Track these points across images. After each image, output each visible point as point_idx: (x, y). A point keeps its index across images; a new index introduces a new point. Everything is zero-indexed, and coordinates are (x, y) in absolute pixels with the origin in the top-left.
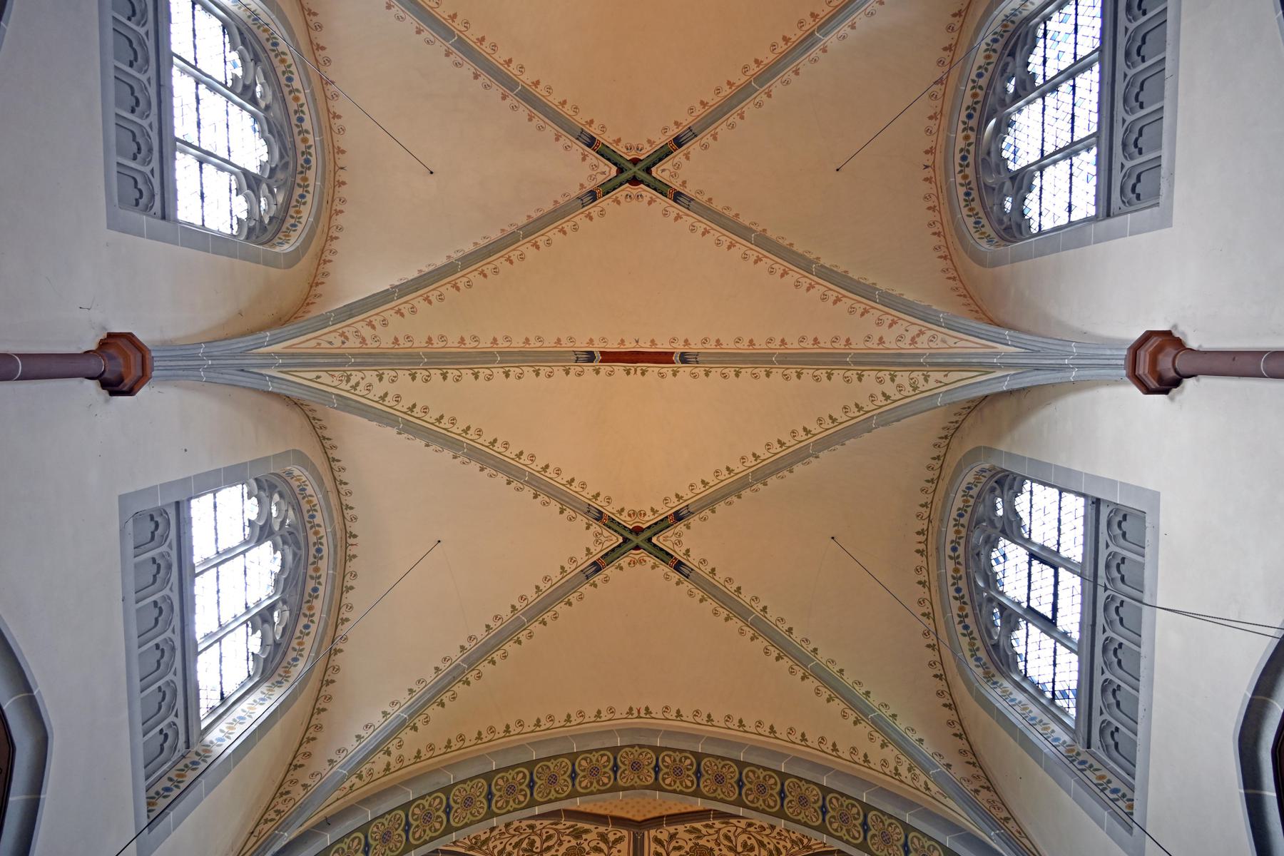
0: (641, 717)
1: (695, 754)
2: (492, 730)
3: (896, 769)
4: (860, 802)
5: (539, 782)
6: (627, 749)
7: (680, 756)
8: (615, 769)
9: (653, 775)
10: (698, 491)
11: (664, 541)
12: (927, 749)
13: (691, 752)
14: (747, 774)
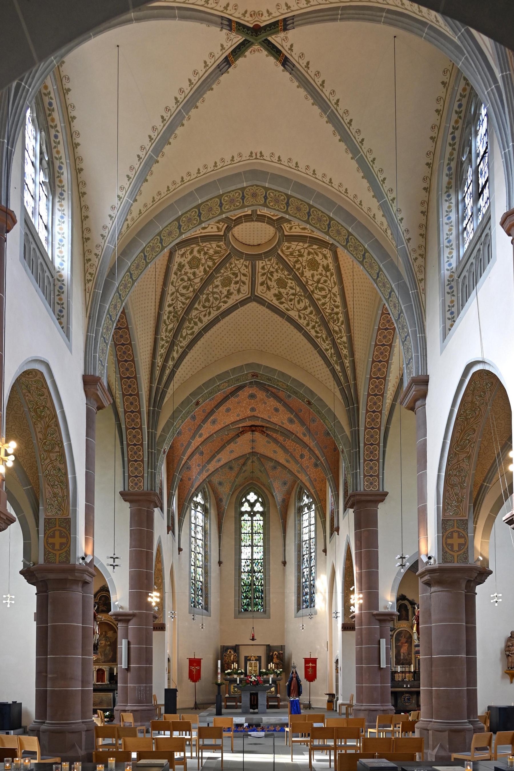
0: (257, 159)
2: (174, 183)
3: (386, 229)
4: (364, 247)
5: (203, 213)
8: (243, 198)
10: (302, 6)
12: (402, 227)
14: (313, 211)
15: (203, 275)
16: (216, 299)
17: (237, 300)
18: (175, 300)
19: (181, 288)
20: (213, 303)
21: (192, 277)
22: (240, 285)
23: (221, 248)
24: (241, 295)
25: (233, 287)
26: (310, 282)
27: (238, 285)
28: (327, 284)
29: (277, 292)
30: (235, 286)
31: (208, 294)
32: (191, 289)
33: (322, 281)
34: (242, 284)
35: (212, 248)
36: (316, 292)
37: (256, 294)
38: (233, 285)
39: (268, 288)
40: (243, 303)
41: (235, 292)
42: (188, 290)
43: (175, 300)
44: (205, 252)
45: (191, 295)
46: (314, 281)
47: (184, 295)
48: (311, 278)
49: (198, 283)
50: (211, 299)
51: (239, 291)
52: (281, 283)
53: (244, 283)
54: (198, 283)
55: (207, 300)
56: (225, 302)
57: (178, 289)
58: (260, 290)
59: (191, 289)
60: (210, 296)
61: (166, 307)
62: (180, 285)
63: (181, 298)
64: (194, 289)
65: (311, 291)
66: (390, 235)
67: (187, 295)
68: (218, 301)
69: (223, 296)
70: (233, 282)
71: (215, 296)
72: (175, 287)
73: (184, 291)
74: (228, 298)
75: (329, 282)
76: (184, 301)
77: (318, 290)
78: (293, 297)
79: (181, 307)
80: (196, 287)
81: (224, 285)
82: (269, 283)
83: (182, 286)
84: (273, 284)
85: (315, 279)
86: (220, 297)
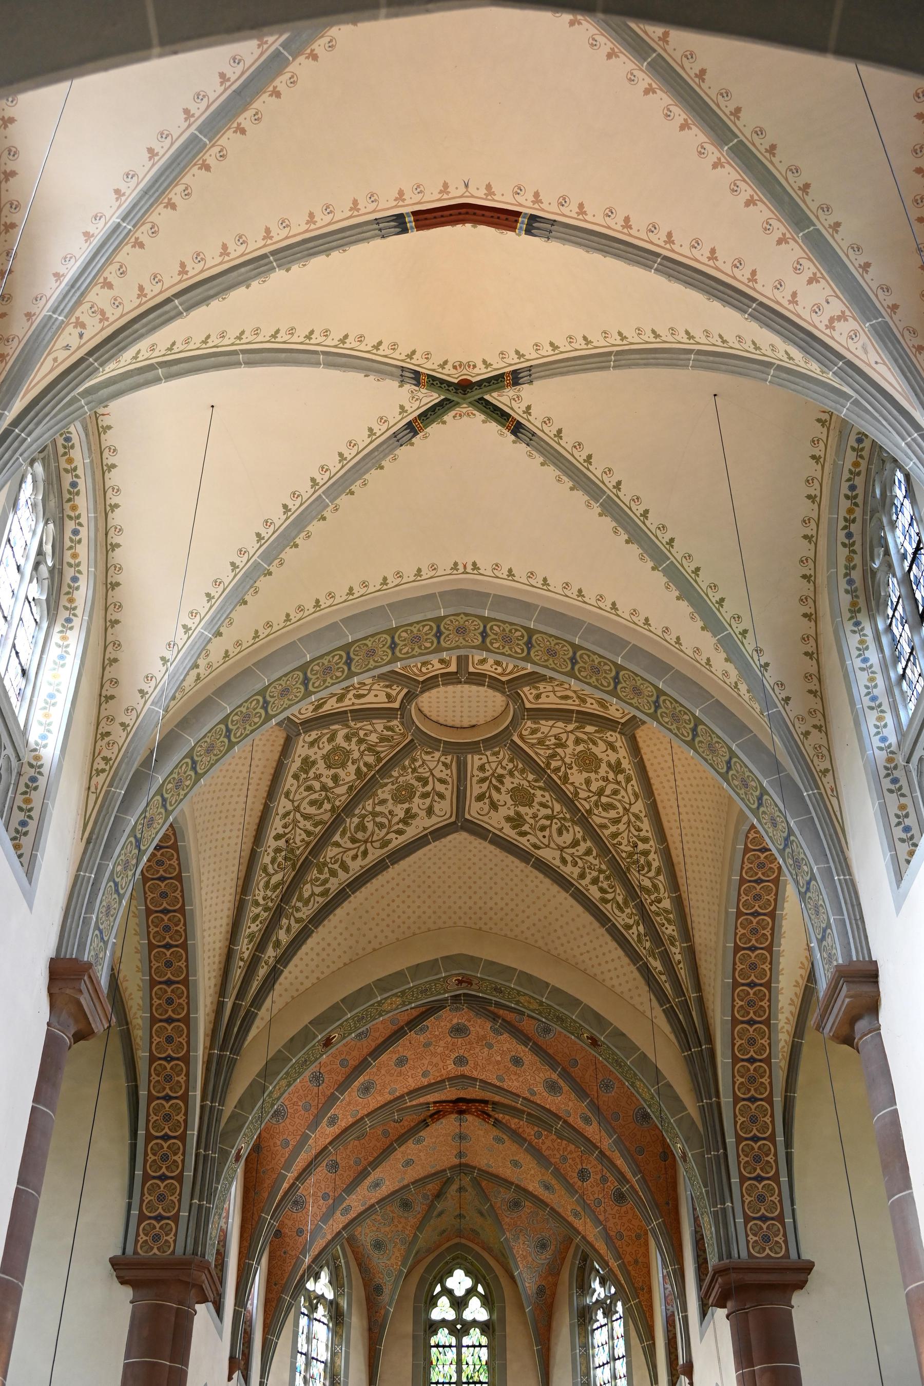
1: (527, 629)
4: (693, 715)
6: (452, 618)
7: (509, 627)
9: (480, 639)
11: (502, 398)
12: (770, 677)
13: (523, 627)
16: (381, 826)
17: (425, 829)
18: (291, 827)
19: (305, 804)
20: (373, 834)
22: (433, 800)
24: (434, 819)
26: (583, 794)
27: (428, 801)
28: (619, 797)
29: (512, 813)
30: (422, 801)
31: (363, 817)
32: (327, 806)
33: (608, 792)
34: (436, 798)
36: (596, 812)
37: (467, 816)
38: (416, 800)
40: (439, 833)
41: (423, 814)
42: (320, 807)
43: (291, 827)
45: (326, 817)
47: (311, 818)
48: (584, 787)
49: (343, 795)
50: (370, 826)
51: (430, 811)
52: (521, 796)
53: (441, 796)
54: (343, 795)
55: (362, 827)
56: (400, 832)
57: (299, 806)
58: (475, 810)
59: (327, 806)
60: (366, 819)
62: (304, 798)
63: (303, 823)
64: (333, 807)
65: (587, 811)
66: (746, 692)
67: (317, 818)
68: (384, 831)
69: (395, 819)
70: (418, 794)
71: (378, 819)
72: (293, 801)
73: (312, 810)
75: (623, 793)
76: (311, 828)
78: (548, 823)
80: (337, 803)
81: (398, 798)
83: (307, 800)
84: (503, 797)
85: (594, 787)
86: (390, 821)
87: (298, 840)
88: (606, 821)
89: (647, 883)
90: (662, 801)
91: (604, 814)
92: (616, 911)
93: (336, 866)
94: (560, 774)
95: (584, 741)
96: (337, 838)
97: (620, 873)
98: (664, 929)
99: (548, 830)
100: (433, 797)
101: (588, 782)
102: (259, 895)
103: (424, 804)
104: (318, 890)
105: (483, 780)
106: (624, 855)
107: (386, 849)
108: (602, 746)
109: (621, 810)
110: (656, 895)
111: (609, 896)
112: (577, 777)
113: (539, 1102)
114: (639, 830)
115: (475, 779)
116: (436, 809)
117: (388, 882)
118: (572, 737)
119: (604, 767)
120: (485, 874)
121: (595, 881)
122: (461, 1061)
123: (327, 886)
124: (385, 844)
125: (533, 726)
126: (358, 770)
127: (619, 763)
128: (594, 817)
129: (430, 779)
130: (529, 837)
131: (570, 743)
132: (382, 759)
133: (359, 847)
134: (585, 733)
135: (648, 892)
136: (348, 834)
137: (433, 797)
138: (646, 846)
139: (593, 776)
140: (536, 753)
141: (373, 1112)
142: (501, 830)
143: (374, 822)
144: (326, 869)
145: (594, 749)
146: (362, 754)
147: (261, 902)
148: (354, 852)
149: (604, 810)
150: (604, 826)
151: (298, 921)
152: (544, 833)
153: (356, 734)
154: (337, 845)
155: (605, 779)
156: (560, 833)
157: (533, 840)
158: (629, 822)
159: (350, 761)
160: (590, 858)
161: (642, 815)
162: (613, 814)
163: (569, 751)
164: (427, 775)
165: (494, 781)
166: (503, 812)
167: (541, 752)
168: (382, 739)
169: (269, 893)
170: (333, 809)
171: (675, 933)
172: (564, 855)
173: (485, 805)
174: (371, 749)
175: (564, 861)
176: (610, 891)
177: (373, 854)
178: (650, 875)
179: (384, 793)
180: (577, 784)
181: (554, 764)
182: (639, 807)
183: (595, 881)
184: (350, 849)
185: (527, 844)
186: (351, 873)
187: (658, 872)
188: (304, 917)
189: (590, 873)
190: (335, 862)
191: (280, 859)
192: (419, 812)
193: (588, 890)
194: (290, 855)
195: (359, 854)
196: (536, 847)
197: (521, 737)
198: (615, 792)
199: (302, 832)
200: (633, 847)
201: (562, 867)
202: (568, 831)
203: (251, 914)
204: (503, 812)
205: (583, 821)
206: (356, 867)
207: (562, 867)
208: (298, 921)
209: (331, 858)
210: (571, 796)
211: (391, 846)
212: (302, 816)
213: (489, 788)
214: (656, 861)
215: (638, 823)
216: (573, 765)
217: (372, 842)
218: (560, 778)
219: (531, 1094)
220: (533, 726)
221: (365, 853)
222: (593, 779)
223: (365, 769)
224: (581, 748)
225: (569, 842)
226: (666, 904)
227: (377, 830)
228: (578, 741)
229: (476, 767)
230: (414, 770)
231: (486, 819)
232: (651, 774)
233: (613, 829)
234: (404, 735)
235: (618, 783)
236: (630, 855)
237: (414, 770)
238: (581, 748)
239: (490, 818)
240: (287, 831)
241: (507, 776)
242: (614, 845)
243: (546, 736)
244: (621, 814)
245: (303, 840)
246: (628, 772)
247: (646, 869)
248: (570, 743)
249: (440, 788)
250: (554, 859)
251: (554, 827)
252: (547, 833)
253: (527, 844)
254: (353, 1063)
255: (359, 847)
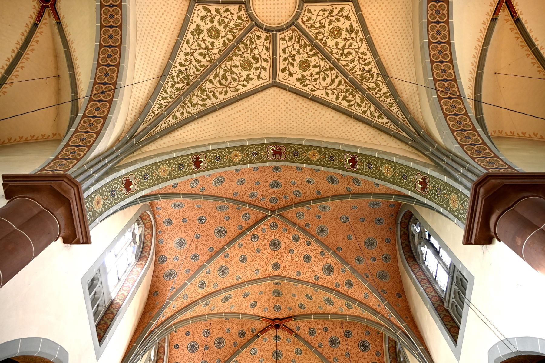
15: (222, 47)
16: (235, 80)
17: (257, 86)
18: (188, 62)
19: (196, 54)
20: (230, 83)
21: (210, 47)
22: (261, 71)
23: (242, 19)
24: (261, 81)
25: (253, 73)
26: (334, 51)
27: (258, 71)
28: (353, 47)
29: (300, 76)
30: (255, 71)
32: (208, 58)
33: (347, 46)
34: (262, 70)
35: (233, 20)
36: (342, 59)
37: (278, 80)
38: (252, 70)
39: (291, 74)
40: (264, 88)
41: (256, 78)
42: (204, 58)
43: (188, 62)
44: (225, 24)
45: (207, 64)
46: (338, 49)
47: (199, 62)
48: (335, 47)
49: (216, 54)
50: (229, 78)
51: (259, 77)
52: (305, 65)
53: (265, 69)
54: (216, 54)
55: (224, 77)
56: (244, 86)
57: (193, 53)
58: (282, 77)
59: (208, 58)
60: (227, 74)
61: (177, 64)
62: (196, 50)
63: (195, 63)
64: (211, 59)
65: (337, 59)
67: (203, 63)
68: (236, 83)
69: (242, 79)
70: (253, 67)
71: (233, 76)
72: (191, 49)
73: (200, 58)
74: (247, 82)
75: (355, 43)
76: (199, 68)
77: (344, 56)
78: (317, 76)
79: (194, 72)
80: (213, 58)
81: (245, 68)
82: (291, 69)
85: (340, 47)
86: (239, 79)
87: (192, 71)
88: (347, 62)
89: (373, 85)
90: (375, 39)
91: (346, 59)
92: (357, 108)
93: (211, 94)
94: (323, 42)
95: (333, 21)
96: (212, 78)
97: (356, 87)
98: (385, 102)
99: (318, 80)
100: (261, 70)
101: (337, 44)
102: (168, 88)
103: (256, 73)
104: (200, 102)
105: (285, 60)
106: (358, 77)
107: (237, 93)
108: (342, 20)
109: (354, 54)
110: (378, 89)
111: (352, 103)
112: (331, 43)
113: (321, 284)
114: (365, 60)
115: (281, 58)
116: (262, 76)
117: (237, 112)
118: (327, 21)
119: (344, 32)
120: (287, 113)
121: (344, 98)
122: (276, 266)
123: (205, 102)
124: (236, 90)
125: (309, 15)
126: (224, 42)
127: (351, 25)
128: (341, 62)
129: (259, 59)
130: (309, 86)
131: (327, 25)
132: (236, 36)
133: (223, 88)
134: (333, 16)
135: (373, 89)
136: (218, 79)
137: (261, 70)
138: (370, 67)
139: (339, 40)
140: (311, 31)
141: (226, 288)
142: (294, 85)
143: (231, 77)
144: (205, 94)
145: (339, 24)
146: (226, 33)
147: (169, 93)
148: (221, 90)
149: (346, 57)
150: (347, 65)
151: (188, 112)
152: (316, 82)
153: (223, 21)
154: (211, 81)
155: (345, 40)
156: (324, 79)
157: (311, 87)
158: (359, 58)
159: (220, 37)
160: (341, 87)
161: (365, 51)
162: (351, 57)
163: (326, 29)
164: (258, 56)
165: (291, 60)
166: (295, 76)
167: (313, 31)
168: (237, 25)
169: (174, 91)
170: (211, 61)
171: (392, 101)
172: (327, 91)
173: (286, 74)
174: (230, 31)
175: (327, 94)
176: (352, 99)
177: (230, 94)
178: (373, 80)
179: (237, 60)
180: (331, 47)
181: (319, 37)
182: (364, 47)
183: (344, 98)
184: (218, 88)
185: (308, 90)
186: (218, 100)
187: (378, 77)
188: (192, 112)
189: (341, 95)
190: (211, 92)
191: (181, 77)
192: (254, 77)
193: (340, 104)
194: (187, 78)
195: (223, 92)
196: (313, 90)
197: (303, 21)
198: (351, 45)
199: (194, 68)
200: (363, 71)
201: (327, 97)
202: (328, 76)
203: (162, 95)
204: (295, 76)
205: (335, 65)
206: (221, 97)
207: (327, 97)
208: (188, 112)
209: (209, 89)
210: (328, 53)
211: (239, 92)
212: (195, 59)
213: (288, 64)
214: (375, 71)
215: (364, 57)
216: (329, 36)
217: (230, 87)
218: (323, 44)
219: (316, 280)
220: (309, 15)
221: (226, 92)
222: (339, 42)
223: (227, 42)
224: (332, 26)
225: (329, 83)
226: (385, 90)
227: (233, 82)
228: (330, 23)
229: (281, 50)
230: (252, 51)
231: (287, 81)
232: (368, 25)
233: (351, 65)
234: (246, 21)
235: (352, 39)
236: (362, 75)
237: (252, 51)
238: (332, 26)
239: (289, 80)
240: (186, 64)
241: (297, 55)
242: (352, 73)
243: (315, 22)
244: (355, 56)
245: (194, 72)
246: (356, 28)
247: (371, 79)
248: (327, 25)
249: (264, 64)
250: (322, 94)
251: (321, 77)
252: (317, 82)
253: (308, 90)
254: (216, 249)
255: (223, 88)
